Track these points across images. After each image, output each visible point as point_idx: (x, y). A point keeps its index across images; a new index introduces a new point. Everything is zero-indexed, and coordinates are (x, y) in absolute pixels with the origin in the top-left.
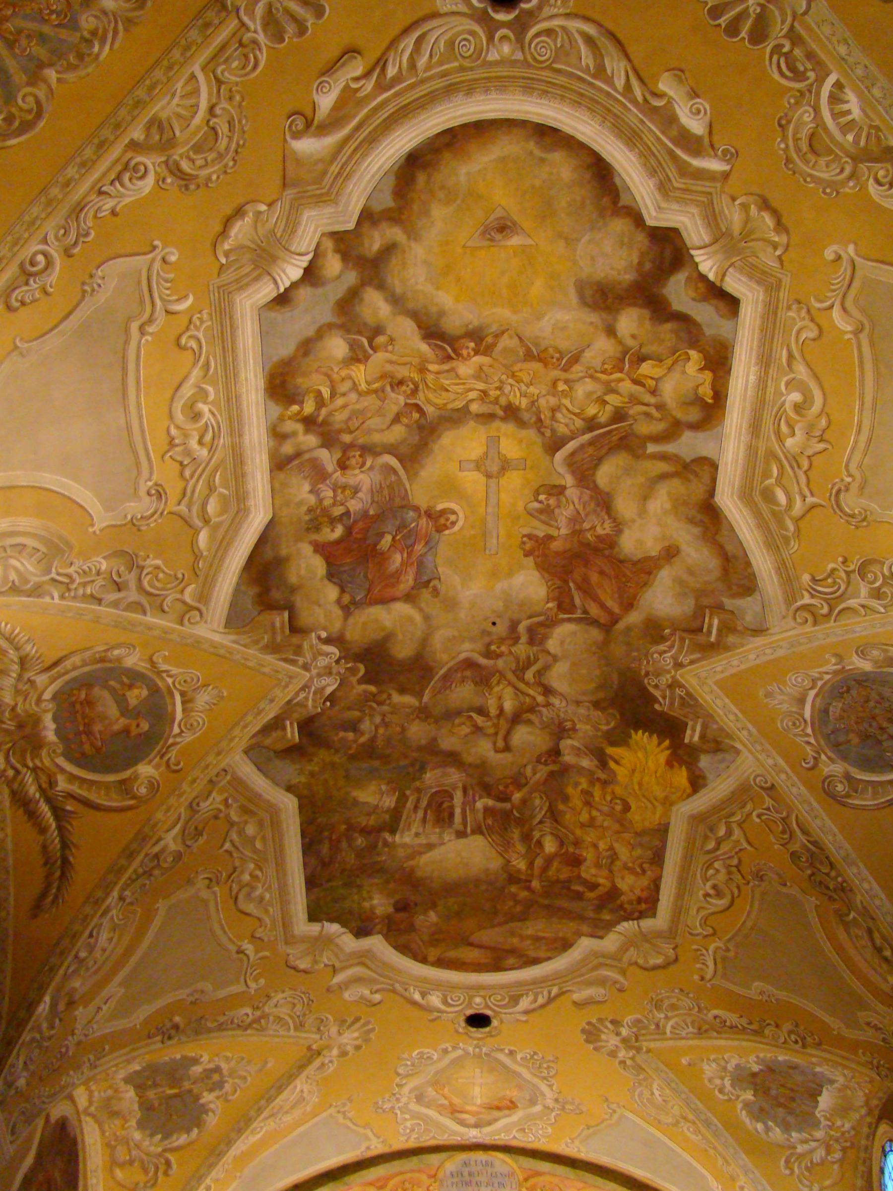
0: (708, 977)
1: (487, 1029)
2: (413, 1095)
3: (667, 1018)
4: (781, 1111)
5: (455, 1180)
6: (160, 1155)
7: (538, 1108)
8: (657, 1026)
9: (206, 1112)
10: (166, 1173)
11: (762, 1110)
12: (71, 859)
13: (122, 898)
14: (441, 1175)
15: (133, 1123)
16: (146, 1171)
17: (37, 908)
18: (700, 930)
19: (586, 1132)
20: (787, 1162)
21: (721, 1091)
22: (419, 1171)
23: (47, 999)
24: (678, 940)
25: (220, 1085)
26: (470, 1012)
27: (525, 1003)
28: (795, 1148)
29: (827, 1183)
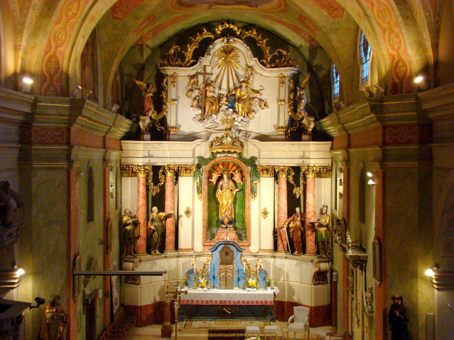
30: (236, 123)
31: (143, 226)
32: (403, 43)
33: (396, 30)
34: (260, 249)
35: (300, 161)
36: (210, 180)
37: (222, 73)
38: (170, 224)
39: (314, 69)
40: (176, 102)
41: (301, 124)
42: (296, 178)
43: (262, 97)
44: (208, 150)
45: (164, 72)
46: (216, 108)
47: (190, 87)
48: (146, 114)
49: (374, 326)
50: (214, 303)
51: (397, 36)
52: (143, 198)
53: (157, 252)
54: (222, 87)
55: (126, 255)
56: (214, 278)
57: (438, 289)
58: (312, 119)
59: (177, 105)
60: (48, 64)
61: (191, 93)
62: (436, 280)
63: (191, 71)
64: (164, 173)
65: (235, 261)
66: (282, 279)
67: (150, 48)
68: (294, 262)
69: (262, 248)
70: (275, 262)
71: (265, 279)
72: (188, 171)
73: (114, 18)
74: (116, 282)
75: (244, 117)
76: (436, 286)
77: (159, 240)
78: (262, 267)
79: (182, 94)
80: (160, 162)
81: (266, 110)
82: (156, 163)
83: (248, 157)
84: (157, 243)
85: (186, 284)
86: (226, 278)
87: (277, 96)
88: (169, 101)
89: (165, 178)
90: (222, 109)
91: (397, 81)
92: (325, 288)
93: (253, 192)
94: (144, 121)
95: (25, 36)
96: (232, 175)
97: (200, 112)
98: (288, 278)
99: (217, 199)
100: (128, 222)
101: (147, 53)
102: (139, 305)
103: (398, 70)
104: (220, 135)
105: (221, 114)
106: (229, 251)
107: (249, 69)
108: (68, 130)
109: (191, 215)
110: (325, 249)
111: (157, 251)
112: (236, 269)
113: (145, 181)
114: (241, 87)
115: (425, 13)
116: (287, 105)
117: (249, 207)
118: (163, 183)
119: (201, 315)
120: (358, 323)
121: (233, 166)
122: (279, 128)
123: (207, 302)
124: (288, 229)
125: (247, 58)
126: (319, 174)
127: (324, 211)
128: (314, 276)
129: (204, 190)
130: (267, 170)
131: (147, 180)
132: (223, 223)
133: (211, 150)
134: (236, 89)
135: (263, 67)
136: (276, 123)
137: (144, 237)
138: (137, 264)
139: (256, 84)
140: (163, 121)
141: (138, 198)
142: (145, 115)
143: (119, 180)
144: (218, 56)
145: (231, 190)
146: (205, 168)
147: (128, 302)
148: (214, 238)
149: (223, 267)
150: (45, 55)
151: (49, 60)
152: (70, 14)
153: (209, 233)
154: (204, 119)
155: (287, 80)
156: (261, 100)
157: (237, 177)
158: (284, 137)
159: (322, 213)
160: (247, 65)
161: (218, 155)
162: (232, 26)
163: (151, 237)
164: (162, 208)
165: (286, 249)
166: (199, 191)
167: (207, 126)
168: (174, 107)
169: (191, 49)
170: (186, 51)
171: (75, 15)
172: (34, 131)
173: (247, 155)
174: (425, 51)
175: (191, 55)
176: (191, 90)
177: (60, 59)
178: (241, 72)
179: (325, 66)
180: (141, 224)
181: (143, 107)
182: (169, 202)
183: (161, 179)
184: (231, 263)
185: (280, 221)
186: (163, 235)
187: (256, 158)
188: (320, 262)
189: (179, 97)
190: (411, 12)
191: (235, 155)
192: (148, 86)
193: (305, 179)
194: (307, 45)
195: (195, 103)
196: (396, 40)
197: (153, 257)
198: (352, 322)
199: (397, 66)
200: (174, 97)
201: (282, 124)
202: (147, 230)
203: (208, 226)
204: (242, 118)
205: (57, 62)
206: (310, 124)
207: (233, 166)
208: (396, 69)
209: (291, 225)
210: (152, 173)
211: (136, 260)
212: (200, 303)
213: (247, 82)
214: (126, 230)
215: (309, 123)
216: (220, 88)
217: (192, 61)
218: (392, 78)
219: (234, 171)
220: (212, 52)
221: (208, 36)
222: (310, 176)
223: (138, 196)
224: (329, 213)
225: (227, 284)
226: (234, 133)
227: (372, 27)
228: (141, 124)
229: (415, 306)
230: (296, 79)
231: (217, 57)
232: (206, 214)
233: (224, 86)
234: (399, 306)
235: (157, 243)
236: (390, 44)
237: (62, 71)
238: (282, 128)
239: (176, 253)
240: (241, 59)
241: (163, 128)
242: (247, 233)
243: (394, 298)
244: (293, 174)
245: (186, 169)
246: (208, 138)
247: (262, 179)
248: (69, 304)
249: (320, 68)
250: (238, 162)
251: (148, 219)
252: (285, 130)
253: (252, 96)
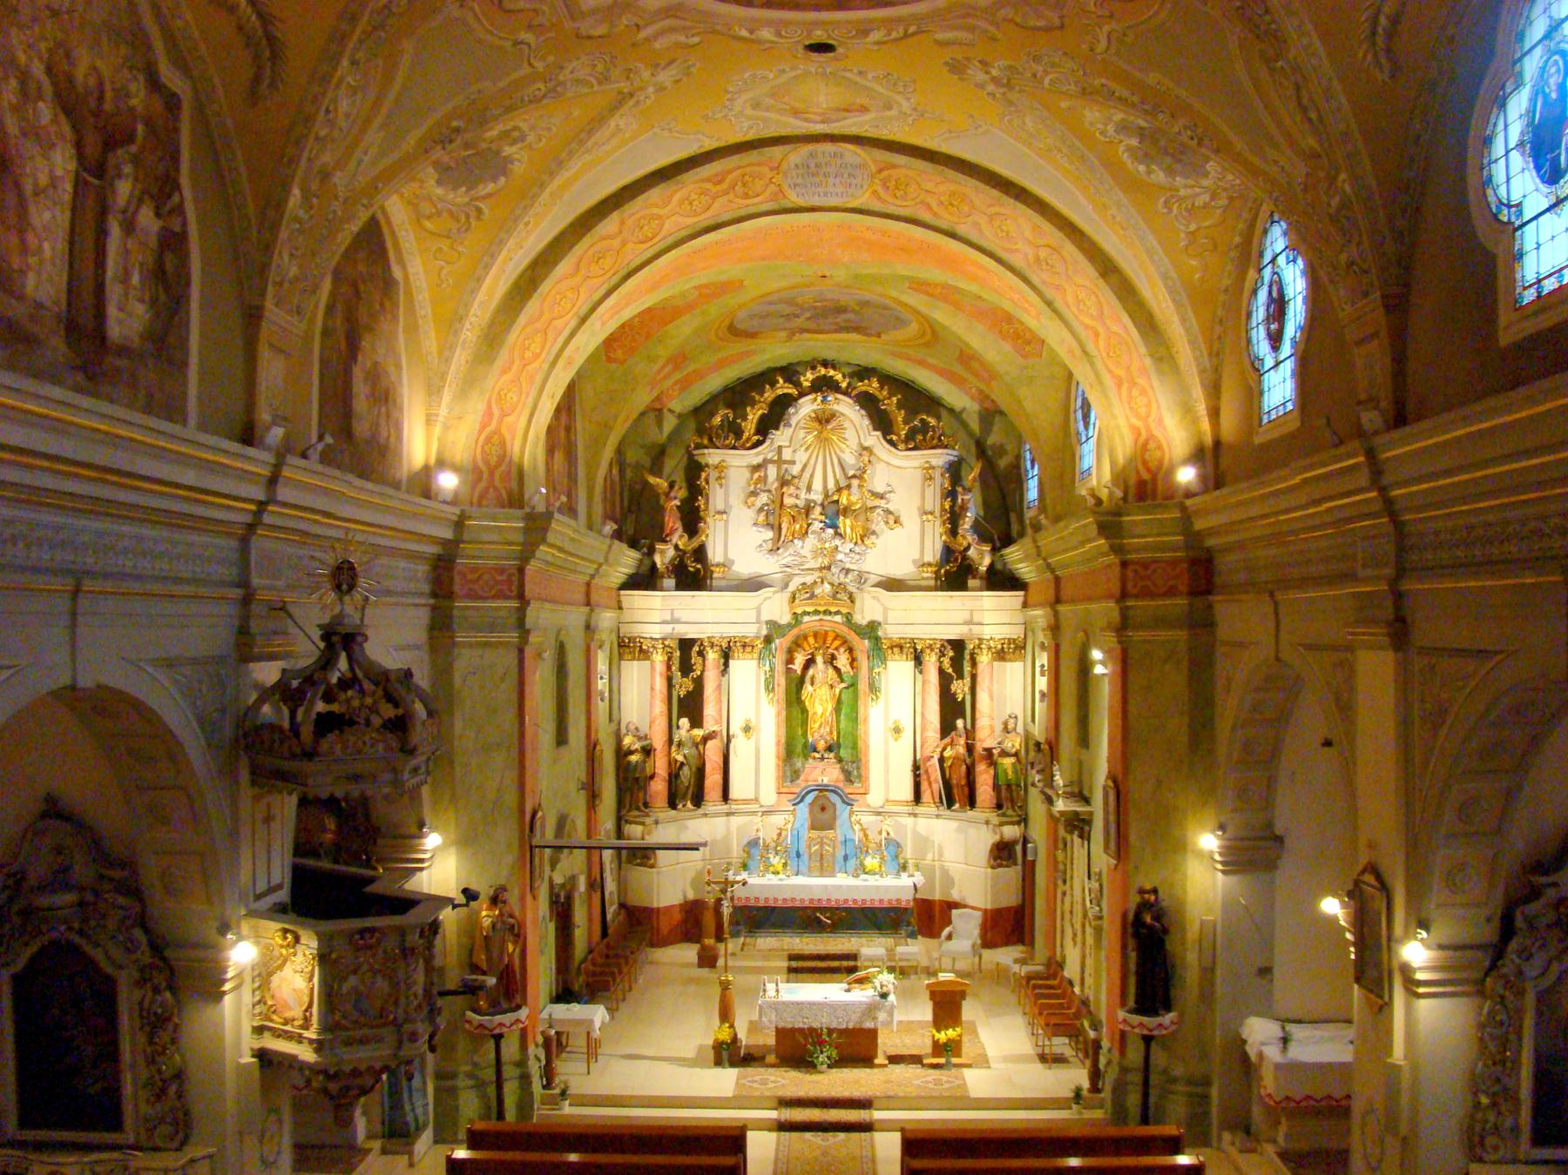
0: (1098, 51)
1: (832, 55)
2: (748, 104)
3: (1046, 73)
4: (1168, 160)
5: (800, 171)
6: (468, 204)
7: (894, 112)
8: (1034, 75)
9: (512, 162)
10: (478, 218)
11: (1146, 155)
12: (279, 35)
13: (354, 63)
14: (784, 166)
15: (432, 182)
16: (458, 221)
17: (253, 97)
18: (1093, 9)
19: (947, 135)
20: (1166, 202)
21: (1101, 133)
22: (759, 164)
23: (296, 191)
24: (1065, 11)
25: (522, 138)
26: (807, 43)
27: (876, 36)
28: (1178, 191)
29: (1207, 224)
30: (840, 557)
32: (1154, 405)
33: (1141, 381)
34: (887, 801)
35: (965, 629)
37: (812, 462)
38: (712, 752)
39: (990, 453)
40: (724, 516)
41: (965, 558)
42: (957, 663)
43: (891, 507)
44: (786, 608)
45: (702, 461)
46: (801, 527)
47: (752, 488)
49: (1105, 943)
50: (798, 904)
51: (1143, 392)
53: (689, 805)
54: (814, 487)
55: (629, 811)
56: (798, 855)
57: (1224, 872)
58: (987, 548)
59: (726, 522)
60: (486, 448)
61: (753, 499)
62: (1220, 854)
63: (754, 457)
64: (701, 654)
65: (838, 822)
66: (929, 856)
68: (954, 825)
69: (892, 797)
70: (915, 825)
71: (897, 857)
73: (609, 360)
74: (611, 862)
75: (856, 543)
76: (1219, 867)
78: (892, 834)
79: (736, 499)
81: (898, 530)
83: (864, 623)
84: (688, 788)
85: (745, 866)
86: (822, 855)
87: (917, 503)
88: (712, 513)
89: (704, 661)
90: (812, 528)
91: (1146, 476)
92: (1012, 874)
93: (874, 689)
94: (663, 552)
95: (447, 397)
96: (833, 657)
97: (770, 534)
98: (941, 855)
99: (803, 702)
100: (633, 748)
101: (670, 423)
102: (655, 905)
103: (1147, 456)
104: (809, 579)
105: (811, 540)
106: (827, 804)
107: (865, 452)
108: (521, 571)
110: (1012, 801)
112: (841, 838)
113: (664, 669)
114: (849, 487)
115: (1193, 350)
116: (938, 522)
117: (866, 720)
119: (774, 926)
120: (1074, 939)
121: (835, 639)
122: (923, 565)
123: (785, 900)
124: (942, 760)
125: (861, 433)
126: (1001, 655)
127: (1010, 727)
128: (991, 851)
130: (901, 647)
131: (669, 668)
132: (815, 750)
133: (791, 608)
134: (839, 490)
135: (893, 449)
136: (917, 556)
139: (878, 480)
140: (700, 553)
142: (664, 541)
143: (615, 667)
145: (832, 686)
147: (635, 900)
148: (798, 777)
149: (814, 834)
150: (480, 432)
151: (488, 440)
152: (528, 354)
155: (937, 474)
156: (888, 512)
157: (843, 661)
158: (932, 583)
159: (1006, 730)
160: (861, 445)
161: (806, 619)
162: (832, 373)
163: (677, 776)
164: (697, 722)
165: (937, 800)
166: (770, 688)
167: (784, 562)
168: (720, 525)
169: (753, 416)
170: (745, 418)
171: (537, 356)
172: (459, 573)
173: (861, 618)
174: (1195, 421)
175: (754, 426)
176: (754, 494)
177: (507, 436)
178: (850, 459)
179: (1009, 447)
181: (662, 527)
184: (831, 827)
185: (926, 745)
186: (700, 773)
187: (879, 624)
188: (1001, 824)
190: (1168, 348)
191: (838, 618)
192: (671, 486)
193: (974, 663)
194: (976, 407)
195: (762, 518)
196: (1141, 401)
197: (683, 814)
198: (1062, 938)
199: (1145, 447)
200: (720, 507)
201: (929, 558)
204: (852, 545)
205: (503, 444)
206: (982, 558)
207: (835, 639)
208: (1143, 455)
209: (947, 754)
210: (678, 653)
211: (648, 821)
212: (771, 903)
213: (860, 477)
214: (629, 762)
215: (981, 554)
216: (809, 489)
217: (756, 438)
218: (1138, 472)
219: (837, 649)
220: (793, 422)
221: (786, 391)
222: (984, 658)
223: (652, 697)
224: (1020, 729)
225: (823, 865)
226: (836, 576)
227: (1097, 376)
228: (658, 559)
229: (1181, 905)
230: (954, 471)
232: (783, 730)
233: (817, 485)
234: (1152, 905)
235: (688, 788)
236: (1131, 408)
237: (510, 461)
238: (930, 565)
239: (725, 808)
240: (850, 434)
241: (699, 566)
242: (863, 768)
243: (1142, 891)
244: (951, 654)
245: (744, 646)
246: (786, 586)
247: (889, 663)
248: (522, 899)
249: (1001, 450)
250: (844, 631)
251: (670, 741)
252: (934, 569)
253: (870, 504)
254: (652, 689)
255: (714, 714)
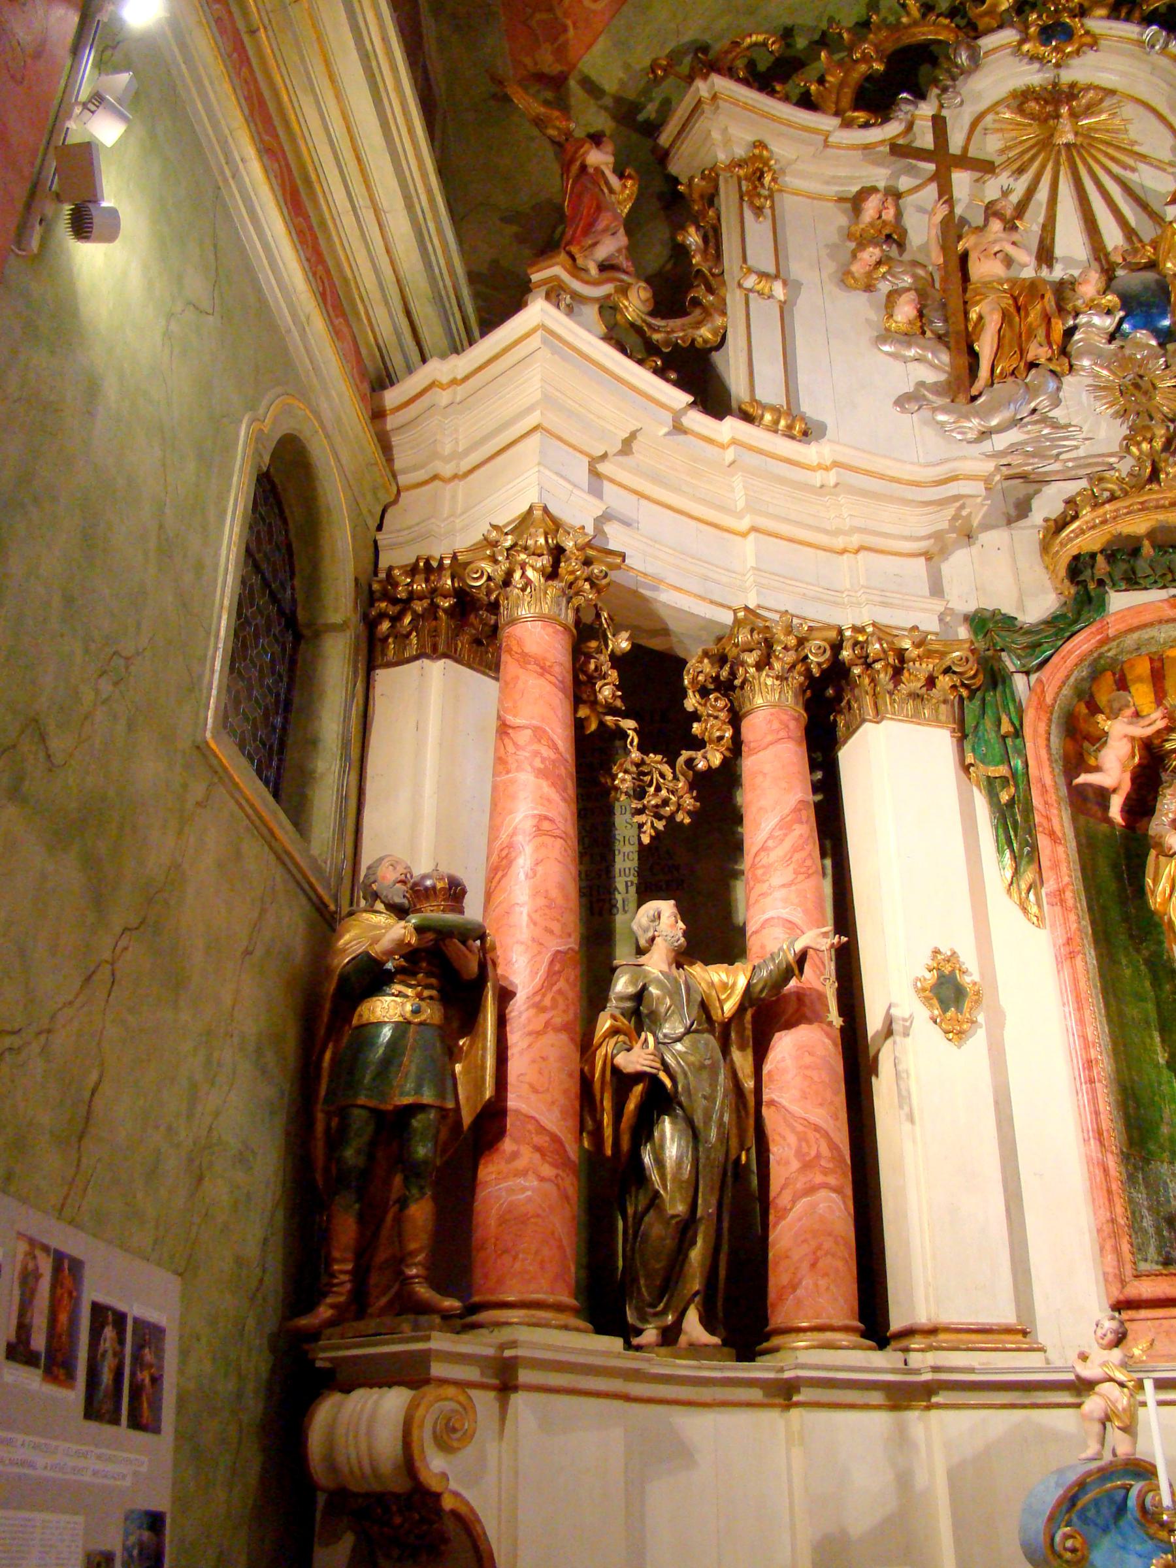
31: (538, 1024)
36: (1083, 778)
37: (1042, 194)
48: (574, 249)
52: (541, 773)
53: (693, 1327)
54: (1058, 252)
59: (785, 310)
61: (871, 254)
67: (608, 101)
72: (913, 682)
77: (706, 1207)
80: (694, 586)
82: (657, 583)
84: (686, 1228)
89: (736, 719)
109: (981, 1018)
111: (692, 1319)
118: (716, 760)
129: (1052, 834)
137: (555, 1139)
138: (468, 1408)
141: (495, 789)
144: (1001, 130)
146: (1038, 691)
153: (1141, 1196)
154: (974, 399)
161: (1119, 601)
167: (1001, 441)
168: (765, 315)
180: (519, 1008)
182: (779, 894)
183: (695, 717)
189: (798, 285)
195: (905, 311)
202: (586, 1082)
203: (1131, 1142)
216: (1045, 255)
231: (999, 135)
246: (1023, 509)
254: (504, 729)
255: (798, 917)
